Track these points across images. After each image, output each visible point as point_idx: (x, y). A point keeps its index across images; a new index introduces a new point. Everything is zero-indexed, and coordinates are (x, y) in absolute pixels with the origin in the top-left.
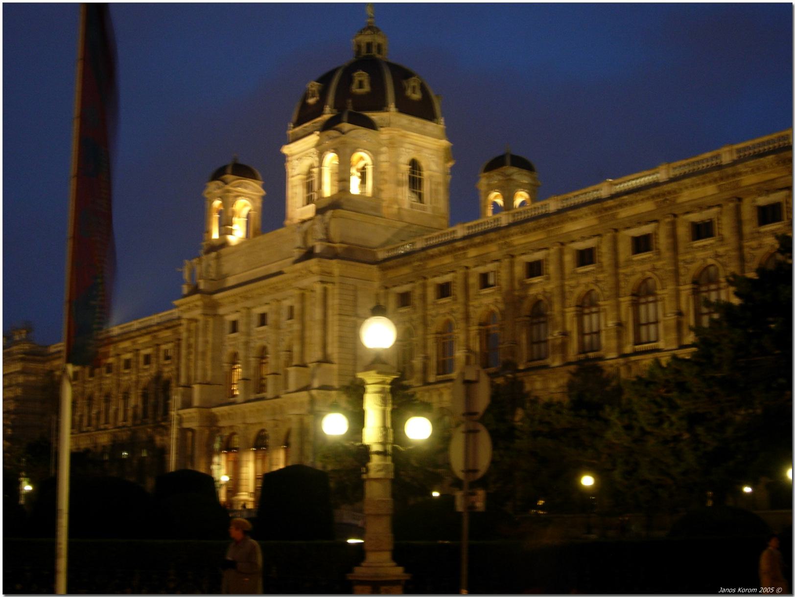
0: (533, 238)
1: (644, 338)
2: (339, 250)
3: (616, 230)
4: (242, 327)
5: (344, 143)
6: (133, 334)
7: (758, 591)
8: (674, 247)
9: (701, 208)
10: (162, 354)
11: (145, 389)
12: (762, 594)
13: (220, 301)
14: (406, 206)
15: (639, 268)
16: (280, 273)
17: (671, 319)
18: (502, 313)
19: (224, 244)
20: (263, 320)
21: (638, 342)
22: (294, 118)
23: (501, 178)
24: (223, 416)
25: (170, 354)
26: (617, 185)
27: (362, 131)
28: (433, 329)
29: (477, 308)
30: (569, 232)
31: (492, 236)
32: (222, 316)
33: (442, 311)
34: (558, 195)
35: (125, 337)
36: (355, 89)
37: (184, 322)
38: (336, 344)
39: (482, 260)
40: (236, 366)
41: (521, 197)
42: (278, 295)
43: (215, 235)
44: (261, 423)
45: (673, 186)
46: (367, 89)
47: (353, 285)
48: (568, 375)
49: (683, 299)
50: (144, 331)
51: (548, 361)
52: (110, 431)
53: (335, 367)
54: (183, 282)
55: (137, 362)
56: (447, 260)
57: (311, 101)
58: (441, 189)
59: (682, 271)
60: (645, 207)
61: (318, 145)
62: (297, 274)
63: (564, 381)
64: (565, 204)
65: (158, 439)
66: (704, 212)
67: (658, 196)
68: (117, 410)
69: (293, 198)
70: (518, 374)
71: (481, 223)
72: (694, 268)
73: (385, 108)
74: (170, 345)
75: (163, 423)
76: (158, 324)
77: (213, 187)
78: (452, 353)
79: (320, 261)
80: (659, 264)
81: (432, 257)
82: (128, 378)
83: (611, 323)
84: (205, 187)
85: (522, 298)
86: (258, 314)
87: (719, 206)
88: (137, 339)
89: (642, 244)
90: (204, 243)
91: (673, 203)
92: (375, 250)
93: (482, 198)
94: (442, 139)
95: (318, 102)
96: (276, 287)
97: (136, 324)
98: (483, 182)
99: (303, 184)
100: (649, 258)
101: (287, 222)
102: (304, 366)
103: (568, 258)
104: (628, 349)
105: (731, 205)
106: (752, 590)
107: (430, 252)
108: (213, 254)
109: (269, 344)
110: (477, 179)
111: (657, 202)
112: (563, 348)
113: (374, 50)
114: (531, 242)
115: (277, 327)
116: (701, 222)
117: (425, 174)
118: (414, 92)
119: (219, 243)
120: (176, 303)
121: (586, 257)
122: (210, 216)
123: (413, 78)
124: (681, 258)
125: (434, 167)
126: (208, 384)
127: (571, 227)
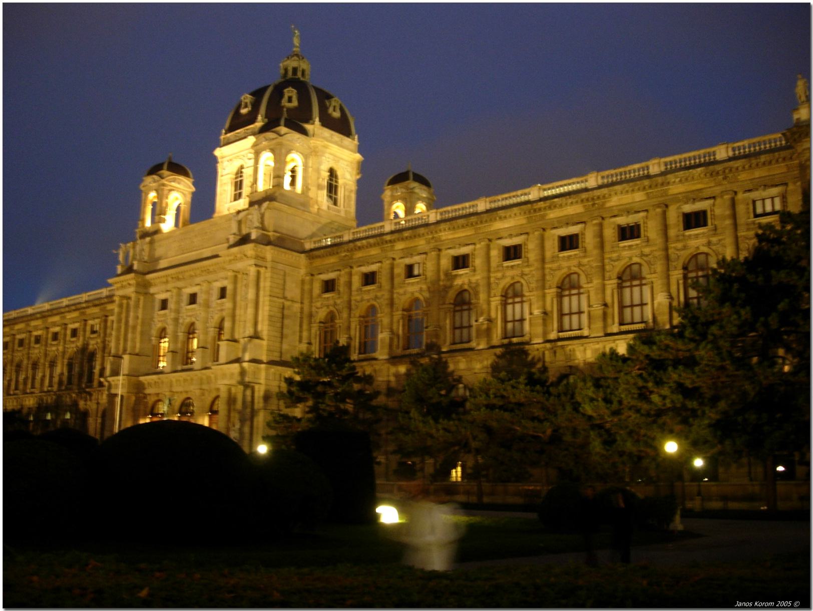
0: (460, 234)
1: (567, 327)
2: (272, 239)
3: (544, 230)
4: (171, 305)
5: (281, 144)
6: (63, 310)
8: (602, 246)
9: (629, 212)
10: (88, 328)
11: (70, 359)
13: (152, 281)
14: (324, 207)
15: (565, 264)
16: (216, 256)
17: (598, 310)
18: (426, 300)
19: (157, 231)
20: (193, 299)
21: (561, 330)
22: (227, 125)
23: (404, 190)
24: (149, 384)
25: (97, 328)
26: (545, 190)
27: (296, 136)
28: (357, 313)
29: (402, 295)
30: (499, 229)
31: (422, 230)
32: (153, 295)
33: (366, 297)
34: (486, 197)
35: (55, 312)
36: (285, 102)
37: (116, 299)
38: (266, 323)
39: (408, 252)
40: (163, 341)
41: (420, 207)
42: (210, 277)
43: (148, 223)
44: (187, 392)
45: (605, 191)
46: (295, 103)
47: (282, 270)
48: (494, 357)
49: (608, 292)
50: (73, 308)
51: (473, 344)
52: (36, 395)
53: (265, 343)
54: (118, 262)
55: (65, 335)
56: (374, 251)
57: (244, 111)
58: (353, 196)
59: (607, 267)
60: (573, 209)
61: (255, 145)
62: (232, 258)
63: (488, 362)
64: (493, 205)
65: (82, 404)
66: (631, 216)
67: (587, 200)
68: (44, 376)
69: (221, 194)
70: (443, 355)
72: (619, 266)
73: (311, 121)
74: (97, 321)
75: (87, 390)
76: (86, 302)
77: (150, 181)
78: (374, 335)
80: (585, 261)
81: (360, 248)
82: (55, 349)
83: (537, 312)
84: (142, 181)
85: (446, 289)
87: (647, 211)
88: (66, 314)
89: (568, 243)
90: (137, 230)
91: (602, 206)
92: (302, 241)
93: (386, 207)
94: (356, 153)
95: (250, 113)
96: (208, 269)
97: (65, 301)
98: (387, 194)
99: (232, 183)
100: (575, 255)
101: (216, 215)
102: (235, 341)
103: (495, 254)
104: (553, 335)
105: (659, 210)
107: (359, 244)
108: (148, 239)
109: (198, 320)
110: (383, 191)
112: (488, 332)
113: (299, 74)
114: (459, 238)
115: (207, 305)
116: (626, 226)
117: (341, 181)
118: (334, 110)
119: (152, 230)
120: (110, 281)
121: (512, 253)
122: (145, 207)
123: (333, 99)
124: (607, 256)
125: (348, 176)
126: (137, 355)
127: (498, 225)
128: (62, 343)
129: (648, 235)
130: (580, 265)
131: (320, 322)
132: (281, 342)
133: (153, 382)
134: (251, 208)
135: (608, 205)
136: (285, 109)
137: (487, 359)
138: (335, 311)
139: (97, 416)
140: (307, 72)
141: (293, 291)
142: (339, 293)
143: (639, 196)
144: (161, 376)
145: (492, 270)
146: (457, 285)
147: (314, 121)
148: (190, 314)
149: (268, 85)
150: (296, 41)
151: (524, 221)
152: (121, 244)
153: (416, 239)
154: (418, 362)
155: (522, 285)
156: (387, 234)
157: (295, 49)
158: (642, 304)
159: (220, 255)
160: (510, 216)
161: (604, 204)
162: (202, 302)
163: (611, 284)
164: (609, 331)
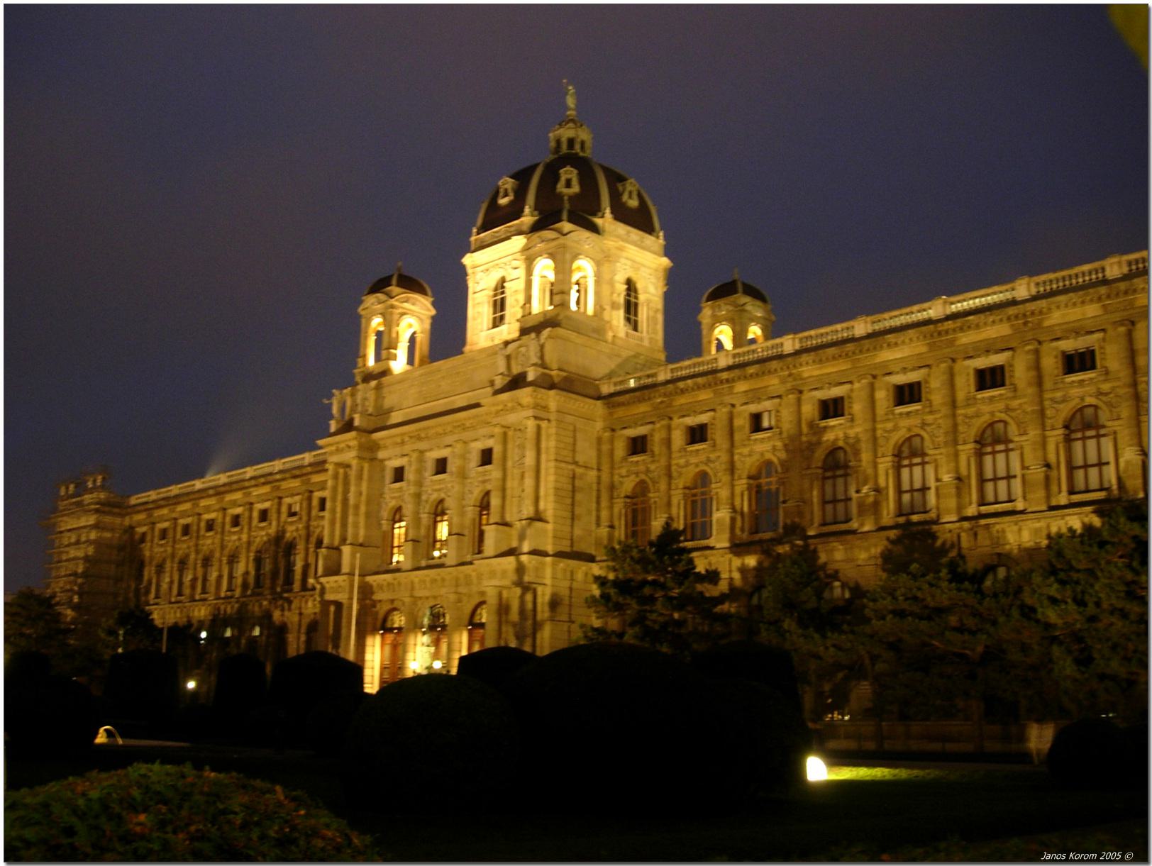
0: (829, 369)
1: (990, 497)
2: (556, 380)
3: (954, 360)
4: (410, 475)
5: (564, 247)
6: (247, 484)
7: (1099, 857)
8: (1039, 381)
9: (1077, 332)
10: (284, 509)
11: (258, 552)
12: (1105, 861)
13: (381, 443)
14: (622, 334)
15: (986, 408)
16: (477, 405)
17: (1037, 472)
18: (782, 463)
19: (386, 372)
20: (441, 466)
21: (982, 502)
22: (479, 221)
23: (731, 308)
24: (381, 587)
25: (296, 508)
26: (952, 303)
27: (583, 234)
28: (680, 483)
29: (745, 456)
30: (888, 361)
31: (774, 365)
32: (382, 461)
33: (693, 460)
34: (867, 315)
35: (235, 486)
36: (561, 188)
37: (330, 467)
38: (551, 498)
39: (754, 396)
40: (397, 525)
41: (755, 331)
42: (466, 435)
43: (371, 362)
44: (435, 597)
45: (1043, 303)
46: (576, 188)
48: (885, 543)
49: (1051, 448)
50: (262, 480)
51: (854, 525)
52: (210, 602)
53: (550, 527)
54: (332, 417)
55: (250, 518)
56: (704, 395)
57: (503, 201)
58: (660, 317)
59: (1049, 413)
60: (996, 330)
61: (526, 249)
62: (500, 407)
63: (876, 550)
64: (877, 327)
65: (277, 615)
66: (1081, 339)
67: (1017, 317)
68: (220, 577)
69: (474, 319)
70: (810, 541)
71: (777, 345)
72: (1065, 410)
73: (600, 214)
74: (297, 498)
75: (286, 595)
76: (280, 472)
77: (371, 301)
78: (706, 512)
79: (535, 391)
80: (1015, 403)
81: (683, 391)
82: (234, 538)
83: (947, 478)
84: (361, 302)
85: (812, 447)
86: (392, 468)
87: (1103, 330)
88: (251, 489)
89: (990, 378)
90: (356, 371)
91: (1039, 325)
92: (597, 382)
93: (705, 332)
94: (662, 257)
95: (511, 203)
96: (463, 424)
97: (250, 472)
98: (706, 313)
99: (489, 302)
100: (1001, 395)
101: (467, 348)
102: (506, 524)
103: (882, 395)
104: (971, 511)
105: (1122, 329)
106: (1089, 856)
107: (681, 385)
108: (373, 383)
109: (449, 496)
110: (699, 310)
111: (1013, 325)
112: (876, 506)
113: (577, 147)
115: (463, 475)
116: (1073, 352)
118: (630, 197)
119: (377, 371)
120: (320, 442)
121: (907, 394)
122: (366, 338)
123: (629, 181)
124: (1047, 395)
125: (652, 289)
126: (361, 545)
127: (886, 355)
128: (246, 530)
129: (1108, 365)
130: (1008, 410)
131: (627, 497)
132: (572, 526)
133: (385, 583)
134: (525, 338)
135: (1046, 323)
136: (566, 198)
137: (876, 546)
138: (648, 480)
139: (299, 631)
140: (588, 144)
141: (587, 453)
142: (653, 455)
143: (1092, 310)
144: (397, 575)
145: (878, 419)
146: (828, 440)
147: (604, 214)
148: (437, 487)
149: (535, 162)
150: (571, 101)
151: (924, 349)
152: (334, 391)
153: (766, 377)
154: (774, 551)
155: (922, 438)
156: (723, 370)
157: (568, 113)
158: (1101, 464)
159: (482, 404)
160: (903, 342)
161: (1040, 322)
162: (454, 469)
163: (1055, 436)
164: (1054, 503)
